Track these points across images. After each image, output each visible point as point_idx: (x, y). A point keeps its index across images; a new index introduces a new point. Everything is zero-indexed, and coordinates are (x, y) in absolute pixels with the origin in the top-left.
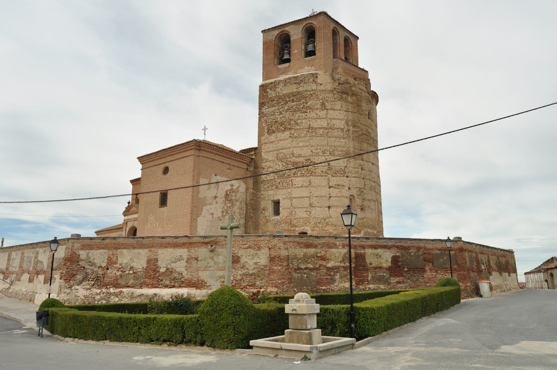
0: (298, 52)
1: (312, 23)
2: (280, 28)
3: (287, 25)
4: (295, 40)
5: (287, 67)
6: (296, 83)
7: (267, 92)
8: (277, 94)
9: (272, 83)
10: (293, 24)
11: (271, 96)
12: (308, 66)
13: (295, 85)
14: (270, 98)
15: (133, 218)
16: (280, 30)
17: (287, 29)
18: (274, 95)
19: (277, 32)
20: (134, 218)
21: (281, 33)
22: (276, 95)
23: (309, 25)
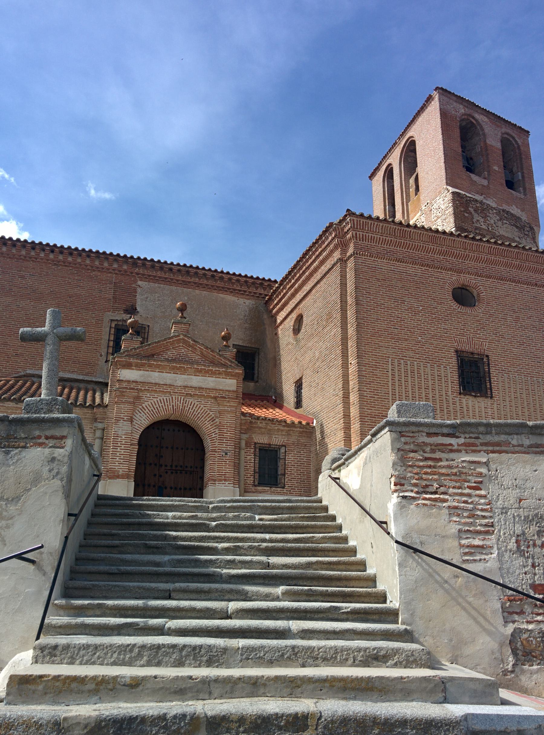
0: (499, 172)
1: (513, 138)
2: (467, 107)
3: (479, 111)
4: (492, 146)
5: (485, 186)
6: (517, 227)
7: (470, 213)
8: (490, 229)
9: (476, 201)
10: (489, 118)
11: (478, 225)
12: (517, 207)
13: (516, 230)
14: (476, 228)
15: (179, 383)
16: (468, 111)
17: (477, 116)
18: (484, 227)
19: (462, 110)
20: (185, 387)
21: (466, 117)
22: (489, 229)
23: (508, 137)
